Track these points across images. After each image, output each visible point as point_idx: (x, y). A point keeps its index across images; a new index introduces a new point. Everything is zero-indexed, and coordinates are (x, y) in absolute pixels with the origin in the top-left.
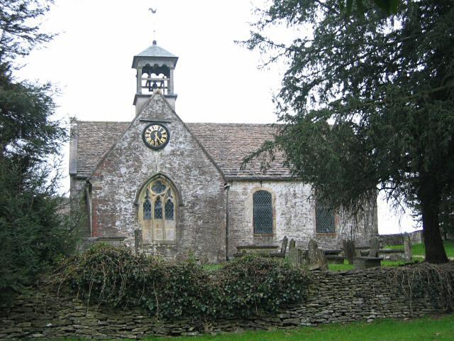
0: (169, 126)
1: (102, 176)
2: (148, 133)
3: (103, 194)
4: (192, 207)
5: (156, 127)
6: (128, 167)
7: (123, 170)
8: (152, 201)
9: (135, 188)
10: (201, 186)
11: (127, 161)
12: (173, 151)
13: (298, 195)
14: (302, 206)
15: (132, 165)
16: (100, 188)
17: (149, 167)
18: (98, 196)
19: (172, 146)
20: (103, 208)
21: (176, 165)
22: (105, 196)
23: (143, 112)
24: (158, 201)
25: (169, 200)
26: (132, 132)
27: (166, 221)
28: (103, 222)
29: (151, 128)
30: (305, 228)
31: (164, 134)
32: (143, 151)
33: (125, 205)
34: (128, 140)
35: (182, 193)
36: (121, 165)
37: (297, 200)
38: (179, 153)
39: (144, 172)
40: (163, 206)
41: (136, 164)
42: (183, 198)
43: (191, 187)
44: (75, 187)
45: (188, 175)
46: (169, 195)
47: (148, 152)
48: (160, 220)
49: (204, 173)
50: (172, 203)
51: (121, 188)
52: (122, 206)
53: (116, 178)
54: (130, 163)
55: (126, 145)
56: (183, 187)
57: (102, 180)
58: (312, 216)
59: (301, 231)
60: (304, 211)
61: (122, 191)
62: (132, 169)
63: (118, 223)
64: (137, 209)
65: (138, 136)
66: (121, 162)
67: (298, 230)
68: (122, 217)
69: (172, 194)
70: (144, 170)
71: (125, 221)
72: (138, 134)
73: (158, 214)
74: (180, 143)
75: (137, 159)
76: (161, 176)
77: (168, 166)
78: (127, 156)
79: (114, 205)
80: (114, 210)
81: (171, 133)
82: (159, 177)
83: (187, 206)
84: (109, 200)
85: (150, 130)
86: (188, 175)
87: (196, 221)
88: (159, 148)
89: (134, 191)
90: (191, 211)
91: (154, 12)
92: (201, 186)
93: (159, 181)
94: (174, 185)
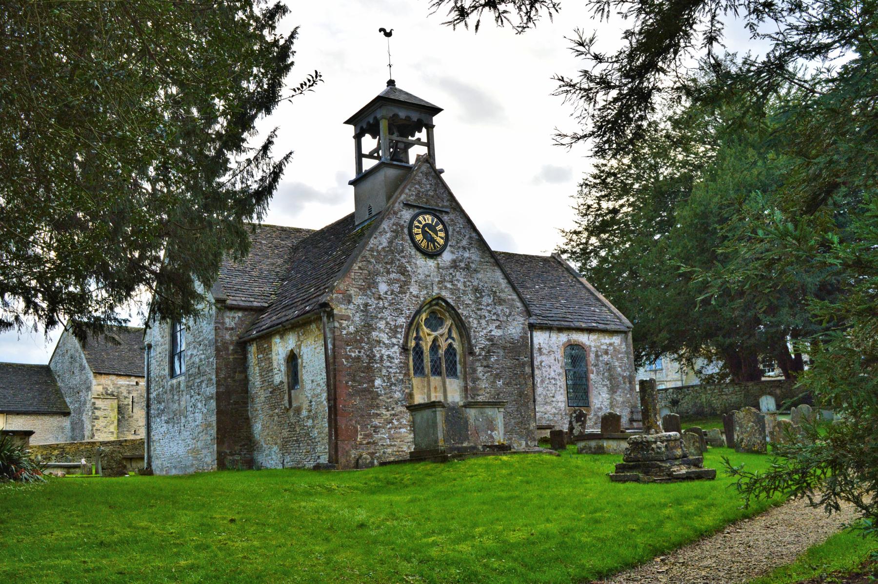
0: (446, 218)
1: (350, 296)
2: (418, 227)
3: (352, 329)
4: (487, 358)
5: (429, 219)
6: (390, 283)
7: (383, 288)
8: (426, 346)
9: (402, 321)
10: (498, 323)
11: (388, 273)
12: (454, 261)
13: (545, 351)
14: (550, 367)
15: (398, 281)
16: (347, 318)
17: (423, 285)
18: (344, 332)
19: (452, 253)
20: (353, 355)
21: (460, 285)
22: (357, 332)
23: (407, 191)
24: (435, 347)
25: (450, 345)
26: (392, 222)
27: (448, 381)
28: (354, 381)
29: (421, 218)
30: (554, 399)
31: (440, 230)
32: (411, 256)
33: (389, 351)
34: (388, 235)
35: (472, 334)
36: (379, 279)
37: (544, 358)
38: (462, 265)
39: (414, 293)
40: (441, 352)
41: (402, 278)
42: (474, 341)
43: (483, 322)
44: (223, 323)
45: (478, 301)
46: (450, 337)
47: (420, 261)
48: (438, 378)
49: (500, 301)
50: (454, 349)
51: (381, 318)
52: (383, 351)
53: (372, 302)
54: (393, 276)
55: (385, 244)
56: (474, 324)
57: (350, 302)
58: (562, 382)
59: (550, 404)
60: (553, 374)
61: (382, 324)
62: (396, 287)
63: (378, 382)
64: (407, 358)
65: (402, 230)
66: (378, 274)
67: (546, 403)
68: (384, 372)
69: (454, 335)
70: (414, 289)
71: (389, 379)
72: (402, 227)
73: (436, 371)
74: (464, 248)
75: (403, 271)
76: (440, 302)
77: (449, 285)
78: (386, 263)
79: (371, 349)
80: (371, 357)
81: (450, 229)
82: (437, 304)
83: (480, 355)
84: (361, 341)
85: (420, 222)
86: (478, 301)
87: (494, 382)
88: (433, 254)
89: (401, 326)
90: (485, 363)
91: (388, 34)
92: (498, 323)
93: (437, 310)
94: (461, 320)
